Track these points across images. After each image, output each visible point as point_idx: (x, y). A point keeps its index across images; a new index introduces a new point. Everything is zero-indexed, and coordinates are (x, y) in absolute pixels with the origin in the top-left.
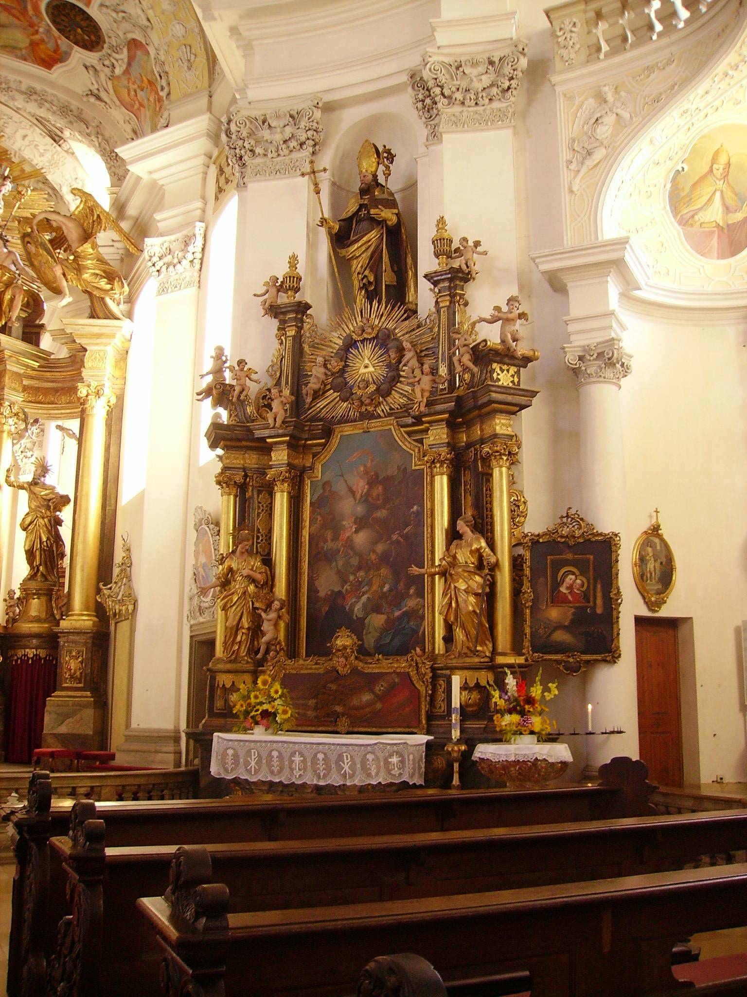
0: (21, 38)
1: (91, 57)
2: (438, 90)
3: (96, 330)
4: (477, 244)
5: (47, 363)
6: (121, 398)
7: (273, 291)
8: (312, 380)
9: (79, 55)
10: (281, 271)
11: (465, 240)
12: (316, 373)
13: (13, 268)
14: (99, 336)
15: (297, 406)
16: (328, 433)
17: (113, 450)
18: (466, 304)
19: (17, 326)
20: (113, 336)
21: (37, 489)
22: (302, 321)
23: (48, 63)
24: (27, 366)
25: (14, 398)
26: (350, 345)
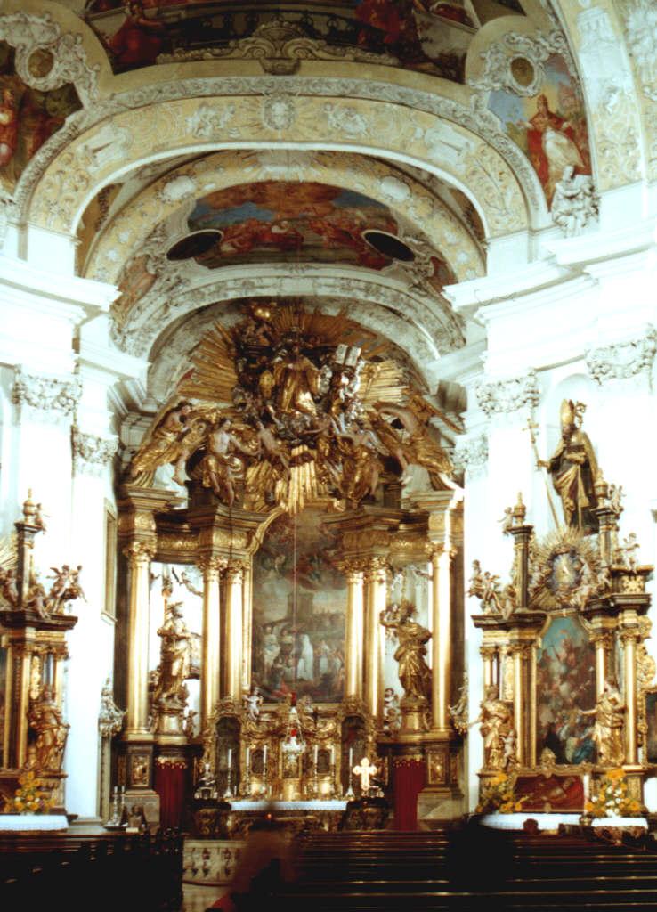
0: (354, 254)
1: (409, 265)
2: (597, 370)
3: (434, 499)
4: (621, 488)
5: (407, 519)
6: (460, 549)
7: (509, 517)
8: (534, 581)
9: (397, 263)
10: (513, 504)
11: (613, 486)
12: (536, 576)
13: (370, 445)
14: (439, 502)
15: (526, 600)
16: (544, 617)
17: (458, 593)
18: (617, 529)
19: (379, 494)
20: (447, 501)
21: (404, 628)
22: (529, 538)
23: (377, 266)
24: (389, 524)
25: (381, 552)
26: (554, 556)
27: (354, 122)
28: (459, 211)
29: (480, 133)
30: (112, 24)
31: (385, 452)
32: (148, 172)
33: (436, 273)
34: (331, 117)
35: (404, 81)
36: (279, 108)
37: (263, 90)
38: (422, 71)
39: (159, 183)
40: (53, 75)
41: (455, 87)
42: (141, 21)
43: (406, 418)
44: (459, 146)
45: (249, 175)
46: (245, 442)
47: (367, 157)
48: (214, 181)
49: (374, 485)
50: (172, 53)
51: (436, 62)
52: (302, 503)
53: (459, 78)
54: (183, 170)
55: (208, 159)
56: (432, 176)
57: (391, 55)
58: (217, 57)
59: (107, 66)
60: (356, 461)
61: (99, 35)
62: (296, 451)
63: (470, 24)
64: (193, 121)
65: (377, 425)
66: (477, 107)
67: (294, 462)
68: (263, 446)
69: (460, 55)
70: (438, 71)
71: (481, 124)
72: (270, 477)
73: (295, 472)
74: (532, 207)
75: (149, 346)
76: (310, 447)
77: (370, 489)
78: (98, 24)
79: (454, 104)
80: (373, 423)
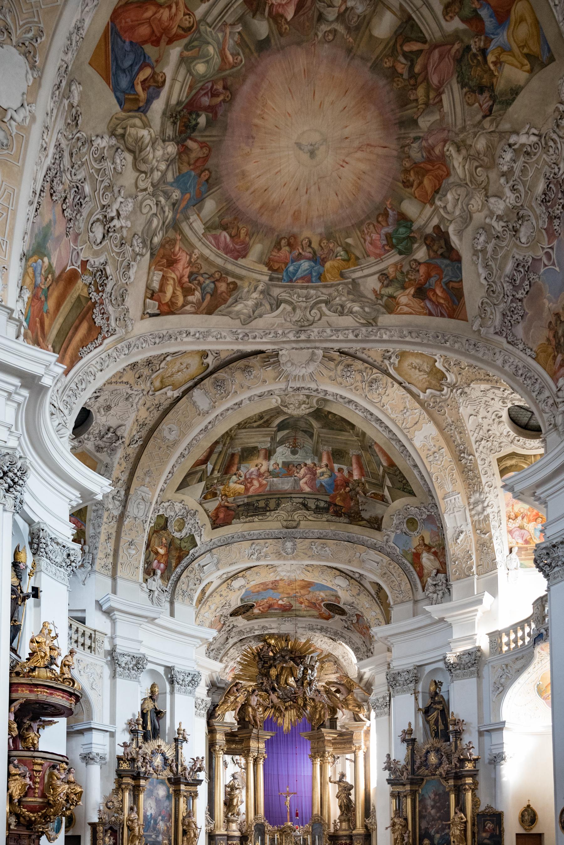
27: (326, 551)
28: (373, 592)
29: (388, 555)
30: (212, 505)
31: (331, 704)
32: (225, 576)
33: (357, 622)
34: (314, 549)
35: (351, 531)
36: (289, 545)
37: (281, 536)
38: (360, 526)
39: (229, 581)
40: (184, 532)
41: (377, 532)
42: (226, 504)
43: (342, 689)
44: (378, 561)
45: (271, 577)
46: (264, 700)
47: (330, 567)
48: (255, 580)
49: (326, 719)
50: (239, 519)
51: (368, 521)
52: (290, 728)
53: (379, 529)
54: (240, 575)
55: (252, 569)
56: (361, 575)
57: (345, 517)
58: (261, 520)
59: (209, 526)
60: (316, 709)
61: (205, 510)
62: (287, 704)
63: (387, 502)
64: (248, 551)
65: (328, 692)
66: (387, 542)
67: (286, 709)
68: (272, 702)
69: (380, 517)
70: (368, 525)
71: (389, 550)
72: (275, 716)
73: (287, 714)
74: (414, 590)
75: (220, 657)
76: (293, 702)
77: (324, 721)
78: (206, 506)
79: (375, 541)
80: (326, 691)
